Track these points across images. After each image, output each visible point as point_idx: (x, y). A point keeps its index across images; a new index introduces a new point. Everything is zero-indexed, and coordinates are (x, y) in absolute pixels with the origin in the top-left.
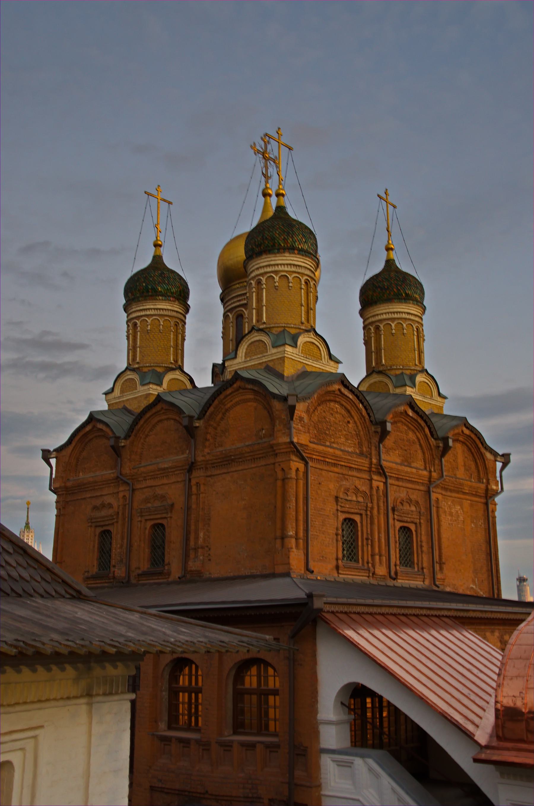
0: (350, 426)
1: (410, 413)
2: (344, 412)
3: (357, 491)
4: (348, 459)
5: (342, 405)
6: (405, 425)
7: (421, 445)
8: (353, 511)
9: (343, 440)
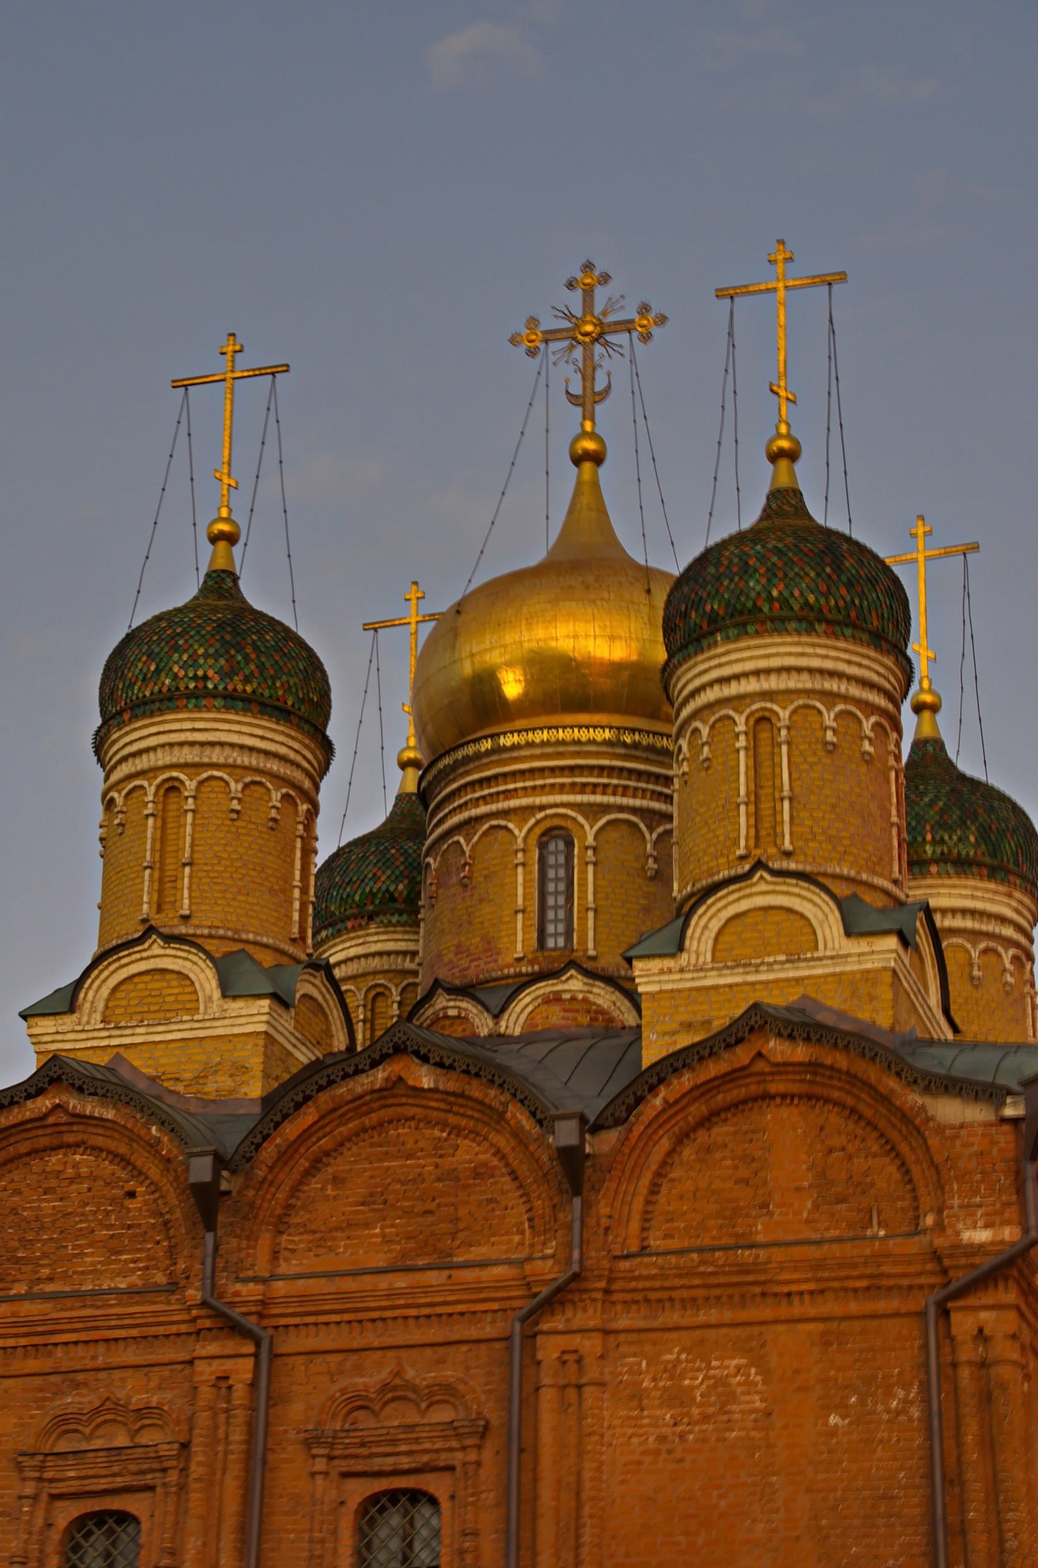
0: (133, 1204)
1: (425, 1078)
2: (108, 1168)
3: (110, 1411)
4: (82, 1319)
5: (96, 1149)
6: (429, 1123)
7: (514, 1175)
8: (103, 1484)
9: (93, 1258)
